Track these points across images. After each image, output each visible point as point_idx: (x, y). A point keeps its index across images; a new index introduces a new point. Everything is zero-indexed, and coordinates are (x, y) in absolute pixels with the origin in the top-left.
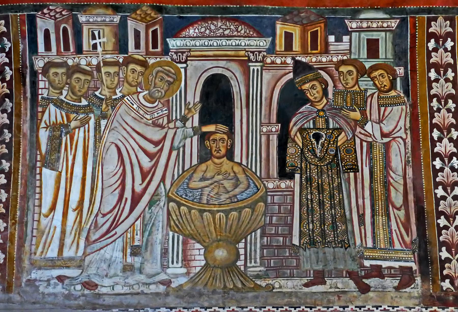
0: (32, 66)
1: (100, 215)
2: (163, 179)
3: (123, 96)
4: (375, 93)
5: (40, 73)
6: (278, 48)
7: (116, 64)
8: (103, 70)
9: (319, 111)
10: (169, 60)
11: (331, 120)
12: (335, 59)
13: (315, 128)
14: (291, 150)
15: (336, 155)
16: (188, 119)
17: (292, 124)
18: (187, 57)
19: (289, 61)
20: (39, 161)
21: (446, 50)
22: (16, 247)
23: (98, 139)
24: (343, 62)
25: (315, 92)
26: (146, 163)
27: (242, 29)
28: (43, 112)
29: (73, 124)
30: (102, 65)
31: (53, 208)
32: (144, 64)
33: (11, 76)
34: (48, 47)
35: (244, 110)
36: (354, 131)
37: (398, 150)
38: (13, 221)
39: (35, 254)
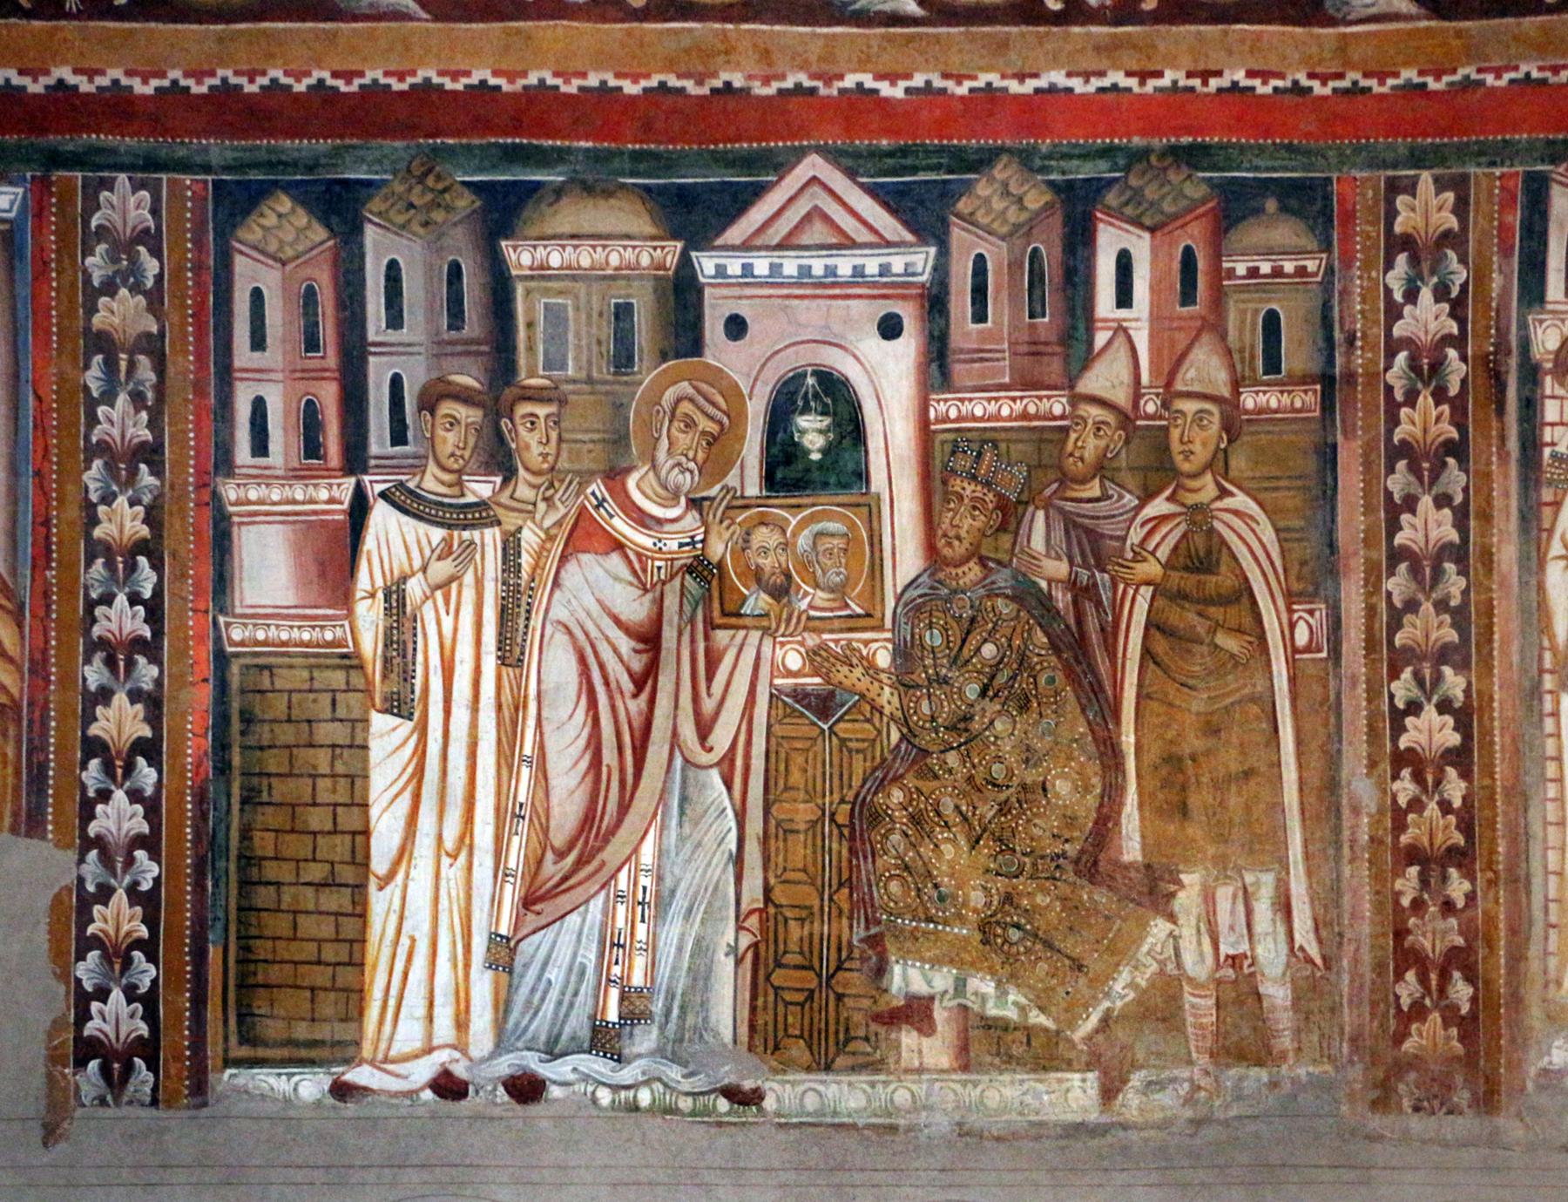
5: (1550, 372)
20: (1551, 672)
22: (1502, 961)
33: (1464, 381)
38: (1490, 875)
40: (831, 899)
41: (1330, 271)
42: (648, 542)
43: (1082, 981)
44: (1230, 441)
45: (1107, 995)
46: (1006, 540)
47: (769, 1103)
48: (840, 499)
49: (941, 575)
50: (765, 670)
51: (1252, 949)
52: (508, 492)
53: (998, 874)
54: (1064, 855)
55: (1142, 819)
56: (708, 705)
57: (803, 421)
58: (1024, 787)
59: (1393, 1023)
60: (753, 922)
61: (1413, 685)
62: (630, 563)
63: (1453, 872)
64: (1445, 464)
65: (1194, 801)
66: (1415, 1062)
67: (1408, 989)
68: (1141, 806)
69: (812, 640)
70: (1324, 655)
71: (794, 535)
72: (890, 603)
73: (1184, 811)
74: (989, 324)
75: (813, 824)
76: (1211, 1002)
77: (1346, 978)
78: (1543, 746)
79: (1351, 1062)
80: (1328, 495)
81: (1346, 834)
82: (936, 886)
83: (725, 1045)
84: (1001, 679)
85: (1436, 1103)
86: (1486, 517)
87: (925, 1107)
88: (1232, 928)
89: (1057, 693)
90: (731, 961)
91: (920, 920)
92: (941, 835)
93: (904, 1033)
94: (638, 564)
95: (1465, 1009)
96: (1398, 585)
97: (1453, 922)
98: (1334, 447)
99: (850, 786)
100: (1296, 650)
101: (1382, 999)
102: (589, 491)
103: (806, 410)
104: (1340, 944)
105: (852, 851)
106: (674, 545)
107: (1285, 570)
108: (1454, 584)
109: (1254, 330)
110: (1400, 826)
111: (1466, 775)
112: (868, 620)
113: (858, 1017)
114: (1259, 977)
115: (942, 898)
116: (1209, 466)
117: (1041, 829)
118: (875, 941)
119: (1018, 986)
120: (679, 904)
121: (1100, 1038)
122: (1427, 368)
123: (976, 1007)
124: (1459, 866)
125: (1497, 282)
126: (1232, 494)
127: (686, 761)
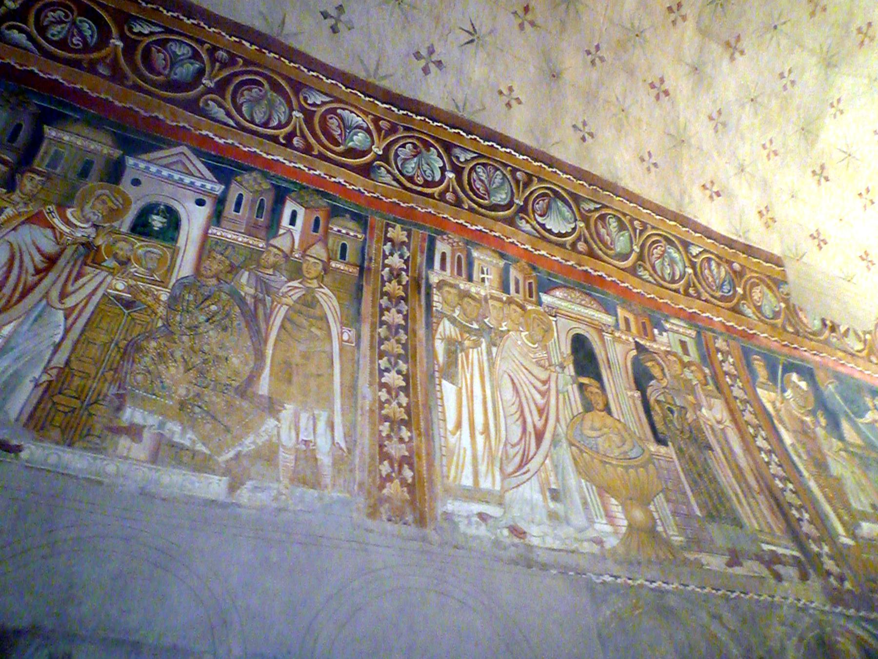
0: (427, 279)
1: (509, 446)
2: (558, 420)
3: (509, 331)
7: (499, 300)
8: (491, 302)
10: (542, 310)
14: (656, 418)
16: (565, 367)
18: (556, 312)
23: (492, 364)
24: (668, 353)
26: (538, 397)
28: (438, 324)
29: (467, 343)
30: (489, 297)
31: (459, 426)
32: (523, 307)
33: (408, 282)
34: (443, 267)
39: (448, 477)
40: (103, 373)
41: (365, 239)
42: (68, 231)
43: (229, 436)
44: (325, 274)
45: (240, 445)
46: (230, 276)
47: (24, 455)
48: (163, 244)
49: (199, 279)
50: (104, 286)
51: (315, 440)
52: (6, 196)
53: (195, 384)
54: (230, 385)
55: (270, 380)
56: (70, 288)
57: (155, 217)
58: (217, 356)
59: (378, 481)
60: (54, 372)
61: (387, 363)
62: (55, 234)
63: (403, 427)
64: (400, 302)
65: (295, 379)
66: (388, 499)
67: (385, 468)
68: (271, 375)
69: (131, 282)
70: (354, 345)
71: (138, 248)
72: (173, 281)
73: (290, 382)
74: (240, 214)
75: (105, 344)
76: (292, 457)
77: (357, 461)
78: (436, 395)
79: (359, 494)
80: (359, 299)
81: (359, 405)
82: (162, 382)
83: (9, 421)
84: (217, 318)
85: (398, 519)
86: (414, 320)
87: (124, 476)
88: (306, 429)
89: (240, 329)
90: (32, 385)
91: (148, 393)
92: (171, 364)
93: (122, 438)
94: (58, 236)
95: (410, 481)
96: (382, 331)
97: (403, 446)
98: (362, 286)
99: (131, 335)
100: (343, 341)
101: (373, 471)
102: (48, 207)
103: (157, 214)
104: (355, 445)
105: (121, 358)
106: (79, 235)
107: (341, 316)
108: (403, 337)
109: (338, 245)
110: (381, 407)
111: (407, 396)
112: (162, 283)
113: (98, 426)
114: (317, 451)
115: (163, 388)
116: (316, 278)
117: (222, 373)
118: (120, 397)
119: (193, 431)
120: (12, 354)
121: (234, 462)
122: (396, 275)
123: (168, 436)
124: (406, 426)
125: (419, 260)
126: (322, 288)
127: (48, 304)
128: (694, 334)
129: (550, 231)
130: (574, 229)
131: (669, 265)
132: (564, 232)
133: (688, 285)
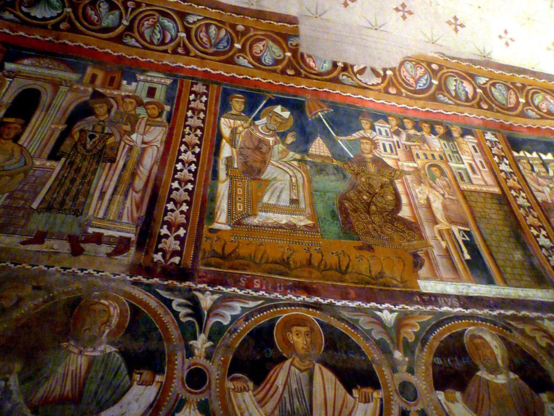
4: (144, 117)
6: (84, 81)
9: (100, 121)
11: (107, 128)
12: (123, 94)
13: (93, 131)
15: (102, 150)
17: (76, 126)
19: (90, 90)
21: (201, 102)
24: (128, 96)
25: (101, 109)
27: (62, 66)
35: (43, 113)
36: (121, 137)
37: (151, 153)
128: (169, 82)
129: (35, 18)
130: (59, 15)
131: (160, 32)
132: (48, 16)
133: (179, 45)
